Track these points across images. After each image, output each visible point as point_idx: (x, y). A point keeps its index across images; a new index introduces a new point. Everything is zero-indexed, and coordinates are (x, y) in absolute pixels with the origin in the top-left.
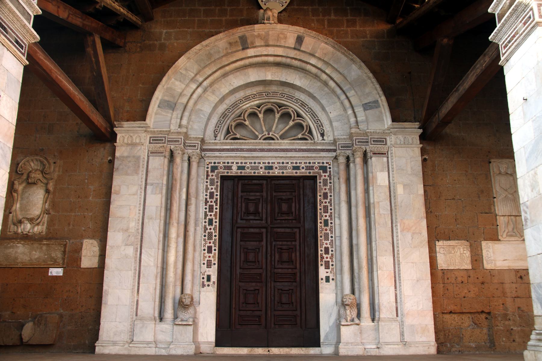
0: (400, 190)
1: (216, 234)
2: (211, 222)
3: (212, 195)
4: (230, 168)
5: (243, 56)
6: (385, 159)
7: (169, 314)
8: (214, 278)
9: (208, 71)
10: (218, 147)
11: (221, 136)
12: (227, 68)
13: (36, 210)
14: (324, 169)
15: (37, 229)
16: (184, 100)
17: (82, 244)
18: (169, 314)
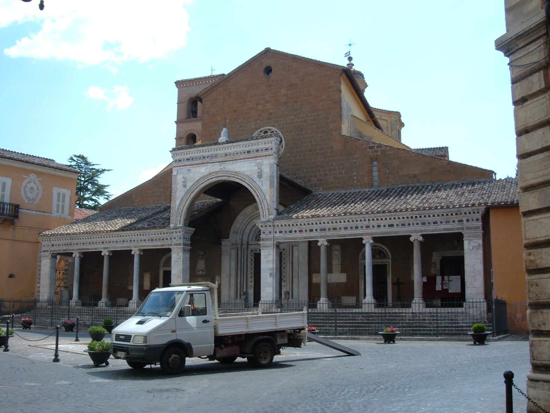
0: (301, 258)
1: (253, 272)
2: (251, 269)
3: (252, 260)
4: (256, 250)
5: (256, 213)
6: (297, 247)
7: (238, 297)
8: (253, 286)
9: (247, 219)
10: (253, 243)
11: (254, 239)
12: (252, 218)
13: (203, 268)
14: (284, 249)
15: (204, 273)
16: (240, 230)
17: (215, 277)
18: (238, 297)
